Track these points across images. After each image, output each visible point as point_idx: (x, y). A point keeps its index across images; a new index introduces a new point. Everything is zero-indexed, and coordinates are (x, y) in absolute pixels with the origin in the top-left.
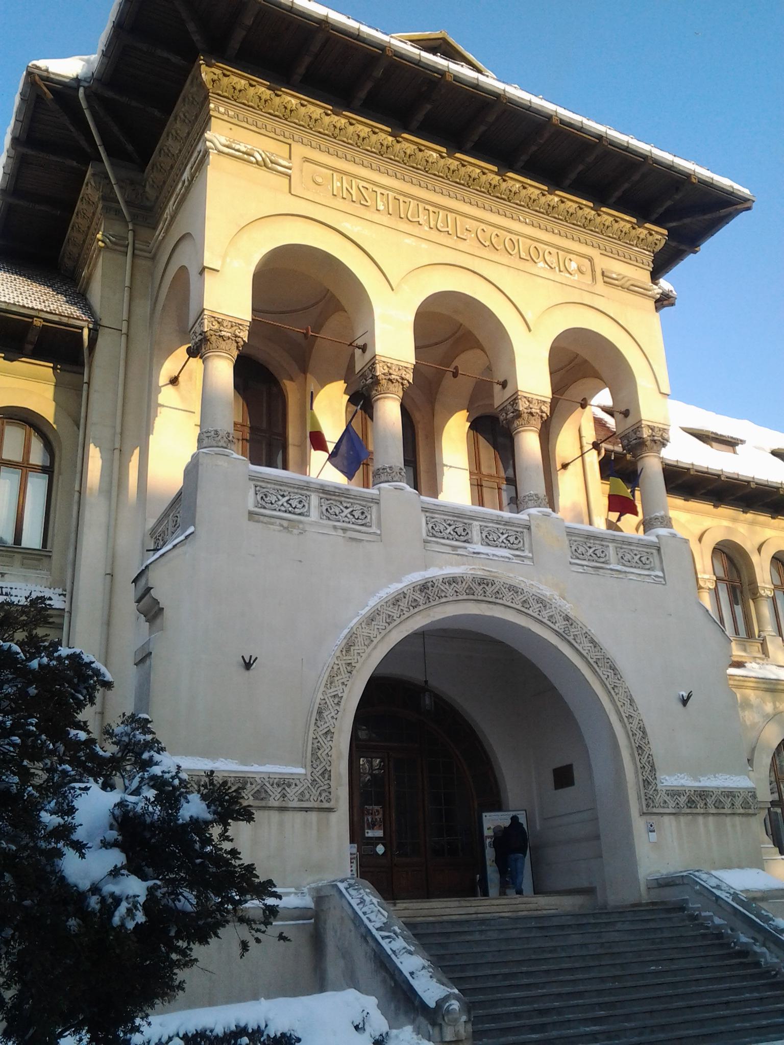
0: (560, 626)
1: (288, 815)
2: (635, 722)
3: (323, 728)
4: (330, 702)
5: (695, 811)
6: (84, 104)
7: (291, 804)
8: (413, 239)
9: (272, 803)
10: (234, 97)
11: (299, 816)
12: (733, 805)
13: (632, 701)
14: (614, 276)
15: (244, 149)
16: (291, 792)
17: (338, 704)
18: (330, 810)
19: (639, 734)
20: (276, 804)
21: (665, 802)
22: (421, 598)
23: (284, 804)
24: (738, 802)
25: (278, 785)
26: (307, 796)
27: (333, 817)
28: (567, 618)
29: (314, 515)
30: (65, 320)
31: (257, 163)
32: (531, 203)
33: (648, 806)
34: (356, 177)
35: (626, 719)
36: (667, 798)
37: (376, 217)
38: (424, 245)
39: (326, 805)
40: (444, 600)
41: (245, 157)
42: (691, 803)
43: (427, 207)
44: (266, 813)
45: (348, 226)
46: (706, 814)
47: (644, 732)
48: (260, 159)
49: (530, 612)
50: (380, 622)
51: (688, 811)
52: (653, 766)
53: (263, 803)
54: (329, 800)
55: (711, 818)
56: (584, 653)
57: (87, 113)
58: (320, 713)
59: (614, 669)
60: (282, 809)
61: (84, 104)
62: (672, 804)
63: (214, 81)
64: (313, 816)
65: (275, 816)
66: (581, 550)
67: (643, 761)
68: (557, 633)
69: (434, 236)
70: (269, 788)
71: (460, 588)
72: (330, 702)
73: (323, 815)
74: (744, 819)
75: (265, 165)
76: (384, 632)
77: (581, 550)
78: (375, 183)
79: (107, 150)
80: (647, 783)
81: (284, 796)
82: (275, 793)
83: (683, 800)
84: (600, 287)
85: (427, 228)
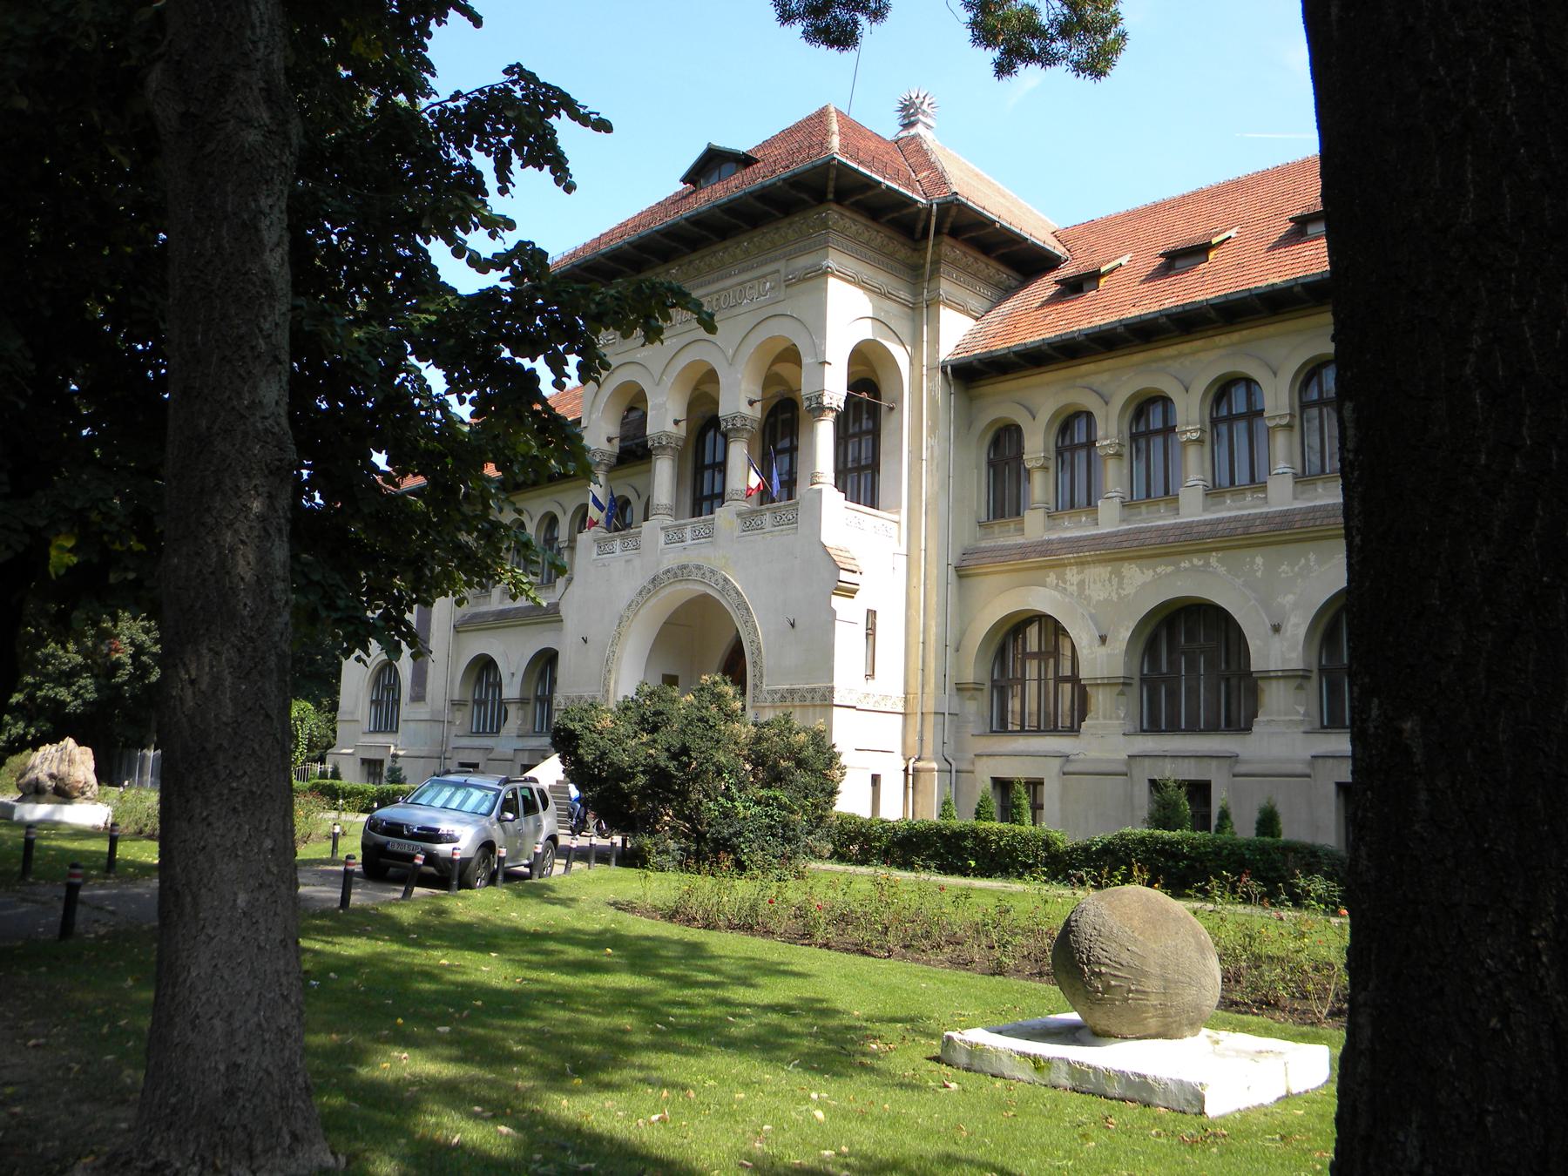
24: (817, 697)
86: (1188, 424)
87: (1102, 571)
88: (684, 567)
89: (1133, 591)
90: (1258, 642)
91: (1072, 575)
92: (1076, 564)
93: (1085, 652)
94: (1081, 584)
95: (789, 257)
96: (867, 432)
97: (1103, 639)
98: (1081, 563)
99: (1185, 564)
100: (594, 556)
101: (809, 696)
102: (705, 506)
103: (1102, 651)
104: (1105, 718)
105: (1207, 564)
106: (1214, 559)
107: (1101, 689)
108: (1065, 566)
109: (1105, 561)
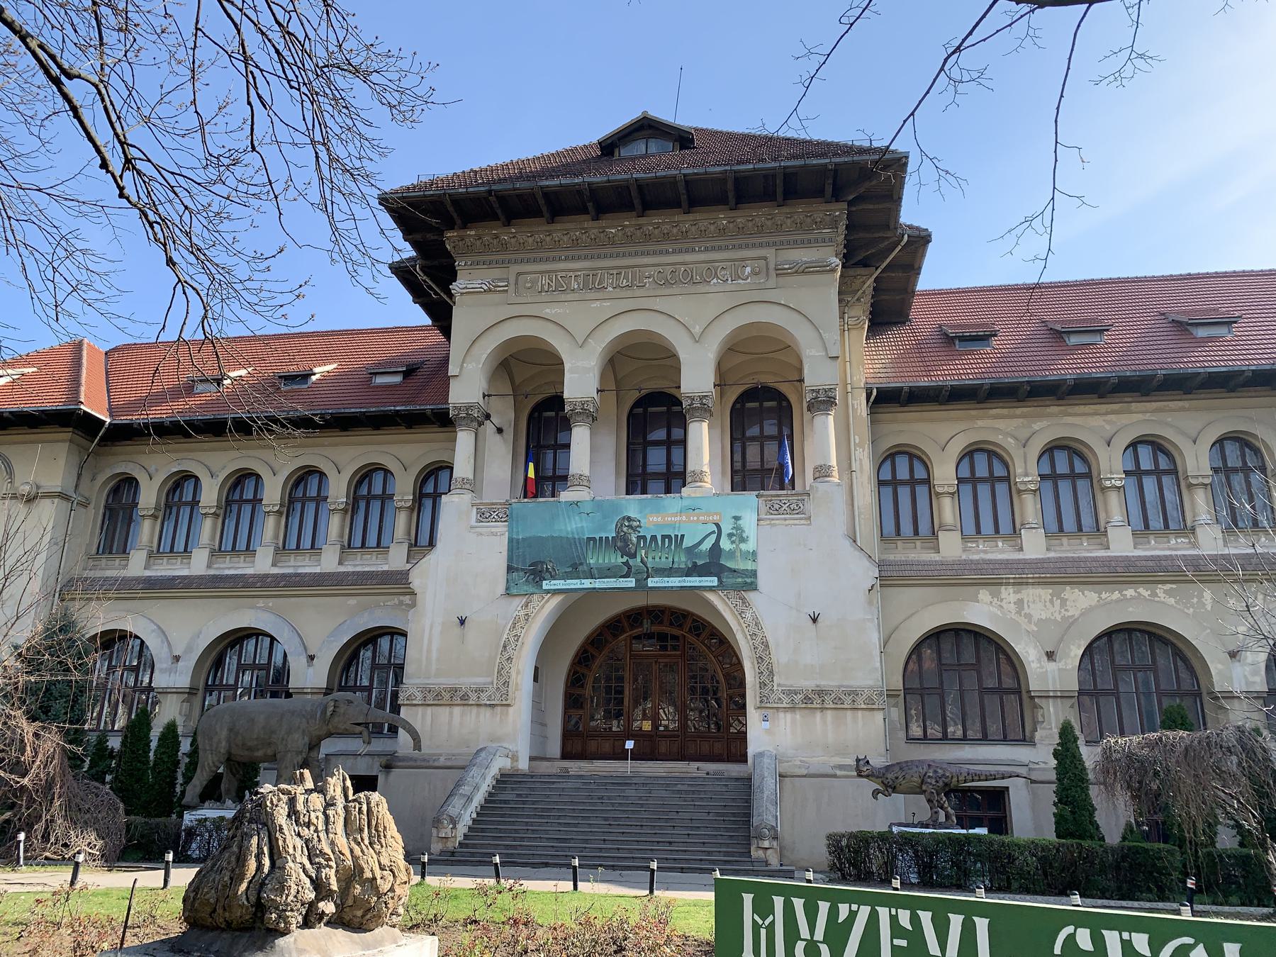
1: (483, 709)
4: (512, 639)
10: (469, 250)
11: (488, 711)
18: (508, 705)
27: (511, 710)
36: (782, 696)
37: (570, 297)
42: (807, 699)
45: (548, 311)
46: (822, 709)
47: (767, 646)
52: (772, 672)
55: (829, 712)
58: (505, 647)
62: (786, 700)
65: (475, 709)
70: (470, 694)
72: (512, 639)
74: (867, 713)
75: (490, 290)
80: (763, 685)
82: (473, 697)
84: (773, 281)
86: (1111, 473)
87: (1045, 593)
89: (1077, 614)
90: (1220, 666)
91: (1008, 594)
92: (1014, 584)
93: (1034, 665)
94: (1020, 603)
95: (780, 246)
96: (771, 438)
97: (1050, 656)
98: (1020, 583)
99: (1130, 592)
100: (473, 523)
102: (548, 487)
103: (1051, 666)
105: (1154, 594)
106: (1161, 590)
107: (1051, 701)
108: (1001, 584)
109: (1046, 583)
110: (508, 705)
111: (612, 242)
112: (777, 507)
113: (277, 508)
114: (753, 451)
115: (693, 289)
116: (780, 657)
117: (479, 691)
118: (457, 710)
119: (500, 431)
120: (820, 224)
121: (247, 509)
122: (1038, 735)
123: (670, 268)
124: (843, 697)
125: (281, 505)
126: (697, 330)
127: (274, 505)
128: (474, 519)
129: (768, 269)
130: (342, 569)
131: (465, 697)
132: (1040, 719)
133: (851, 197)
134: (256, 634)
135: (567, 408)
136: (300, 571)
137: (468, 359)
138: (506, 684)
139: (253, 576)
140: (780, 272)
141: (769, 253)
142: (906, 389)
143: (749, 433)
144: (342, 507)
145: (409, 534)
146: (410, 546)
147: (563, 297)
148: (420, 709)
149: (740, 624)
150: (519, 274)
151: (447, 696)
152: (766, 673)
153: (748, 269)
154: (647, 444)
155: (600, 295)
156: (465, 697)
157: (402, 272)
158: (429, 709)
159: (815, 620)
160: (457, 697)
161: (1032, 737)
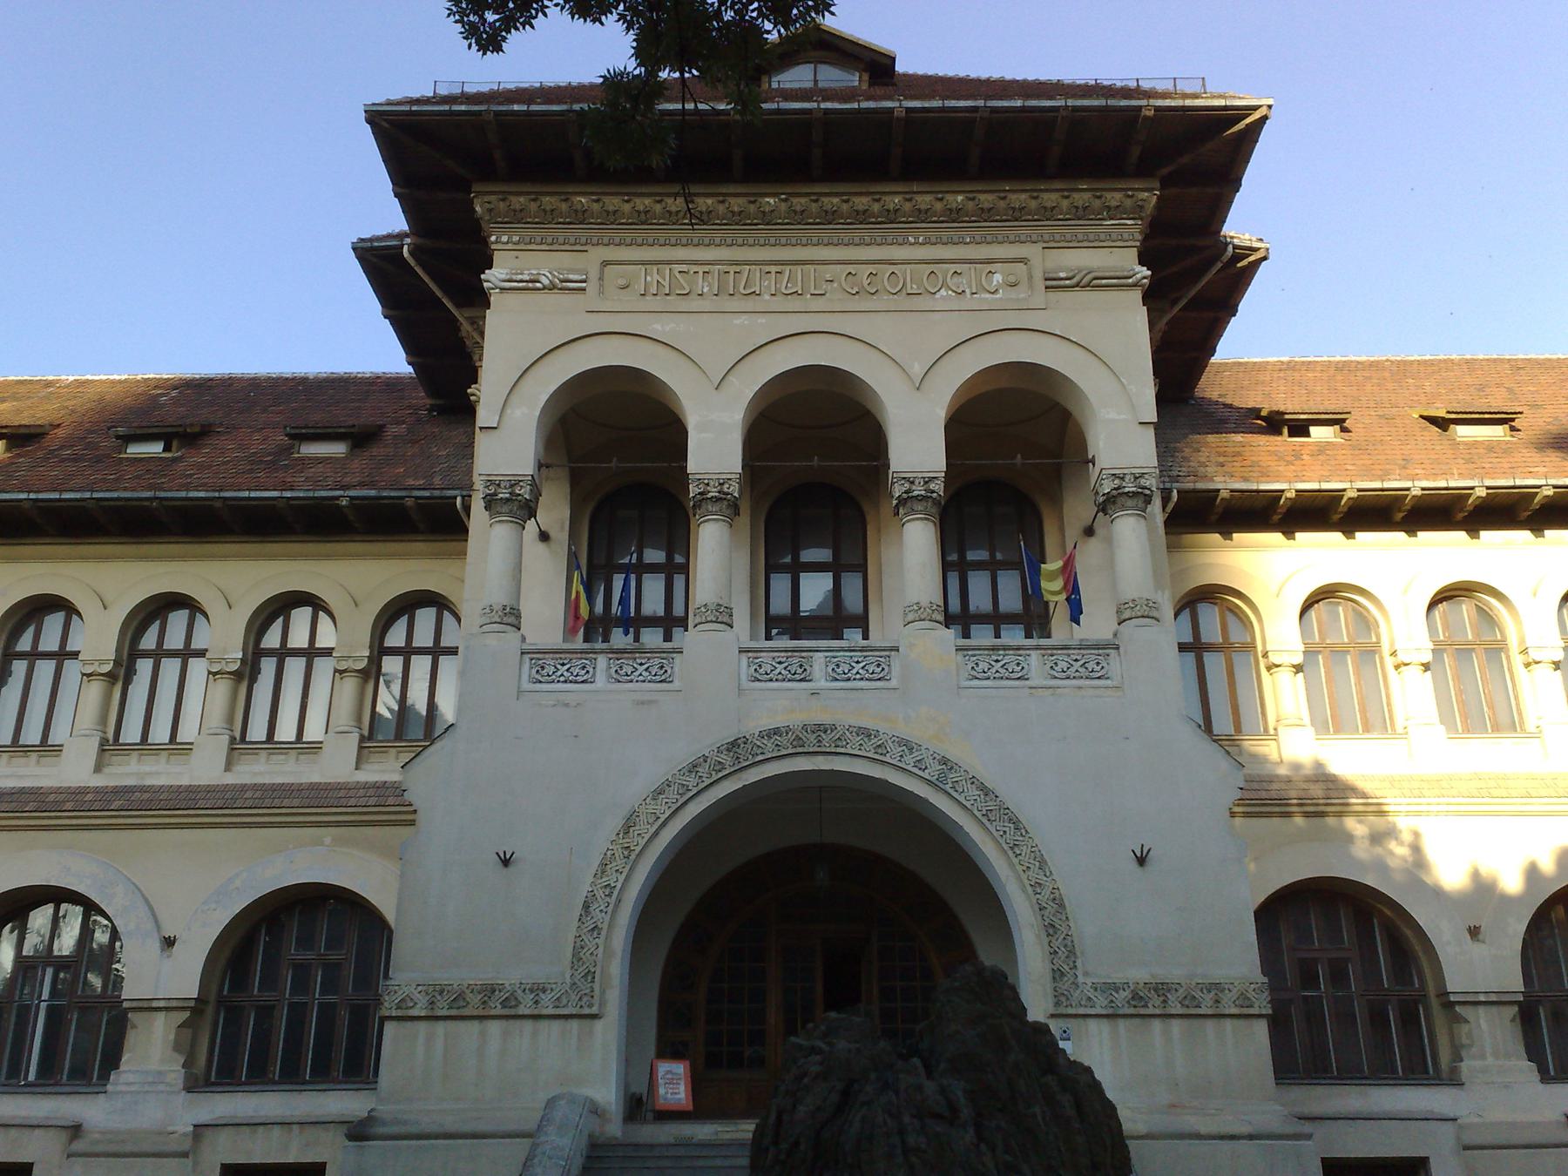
0: (932, 772)
1: (544, 1024)
2: (1046, 893)
3: (590, 924)
4: (600, 893)
5: (1143, 1011)
6: (412, 262)
7: (545, 1012)
8: (745, 317)
9: (522, 1010)
10: (517, 218)
11: (556, 1025)
12: (1217, 1001)
13: (1043, 864)
14: (1062, 275)
15: (526, 277)
16: (546, 998)
17: (609, 895)
18: (594, 1017)
19: (1051, 908)
20: (527, 1012)
21: (1089, 999)
22: (726, 759)
23: (536, 1012)
25: (532, 991)
26: (564, 1001)
27: (599, 1025)
28: (944, 761)
29: (601, 681)
30: (437, 493)
31: (544, 288)
32: (922, 216)
33: (1057, 1004)
34: (669, 263)
35: (1030, 889)
38: (762, 319)
39: (586, 1011)
40: (760, 758)
41: (531, 286)
43: (767, 268)
44: (518, 1022)
45: (657, 327)
47: (1062, 905)
48: (546, 282)
49: (887, 759)
50: (672, 794)
51: (1132, 1011)
53: (512, 1012)
54: (591, 1006)
55: (1176, 1023)
56: (968, 804)
57: (418, 270)
58: (586, 906)
59: (1016, 823)
60: (536, 1017)
61: (412, 262)
63: (490, 210)
64: (574, 1025)
65: (528, 1025)
66: (983, 666)
67: (1055, 944)
68: (929, 782)
69: (779, 303)
71: (783, 740)
72: (600, 893)
73: (586, 1022)
74: (1241, 1022)
76: (674, 807)
77: (983, 666)
78: (696, 263)
79: (452, 299)
80: (1057, 975)
81: (536, 1002)
83: (1125, 994)
84: (1040, 297)
85: (767, 297)
88: (820, 729)
101: (1208, 999)
103: (1477, 950)
104: (1496, 1055)
107: (1481, 1010)
110: (594, 1017)
111: (767, 219)
112: (1064, 665)
113: (107, 668)
114: (979, 584)
115: (903, 302)
116: (1086, 924)
117: (538, 989)
118: (494, 1027)
119: (544, 537)
120: (1114, 212)
121: (45, 669)
122: (1465, 1067)
123: (866, 270)
124: (1198, 994)
125: (117, 663)
126: (917, 370)
127: (102, 662)
128: (525, 677)
129: (1030, 277)
130: (230, 779)
131: (510, 1001)
132: (1465, 1041)
133: (1165, 171)
134: (57, 896)
135: (693, 490)
136: (148, 782)
137: (514, 399)
138: (589, 975)
139: (58, 791)
140: (1054, 284)
141: (1031, 251)
142: (1224, 494)
143: (971, 556)
144: (234, 667)
145: (359, 719)
146: (362, 739)
147: (683, 305)
148: (422, 1027)
149: (1012, 865)
150: (605, 263)
151: (474, 1000)
152: (1062, 953)
153: (998, 278)
154: (796, 569)
155: (749, 304)
156: (510, 1001)
157: (377, 260)
158: (440, 1028)
159: (1141, 861)
160: (493, 1004)
161: (1454, 1071)
